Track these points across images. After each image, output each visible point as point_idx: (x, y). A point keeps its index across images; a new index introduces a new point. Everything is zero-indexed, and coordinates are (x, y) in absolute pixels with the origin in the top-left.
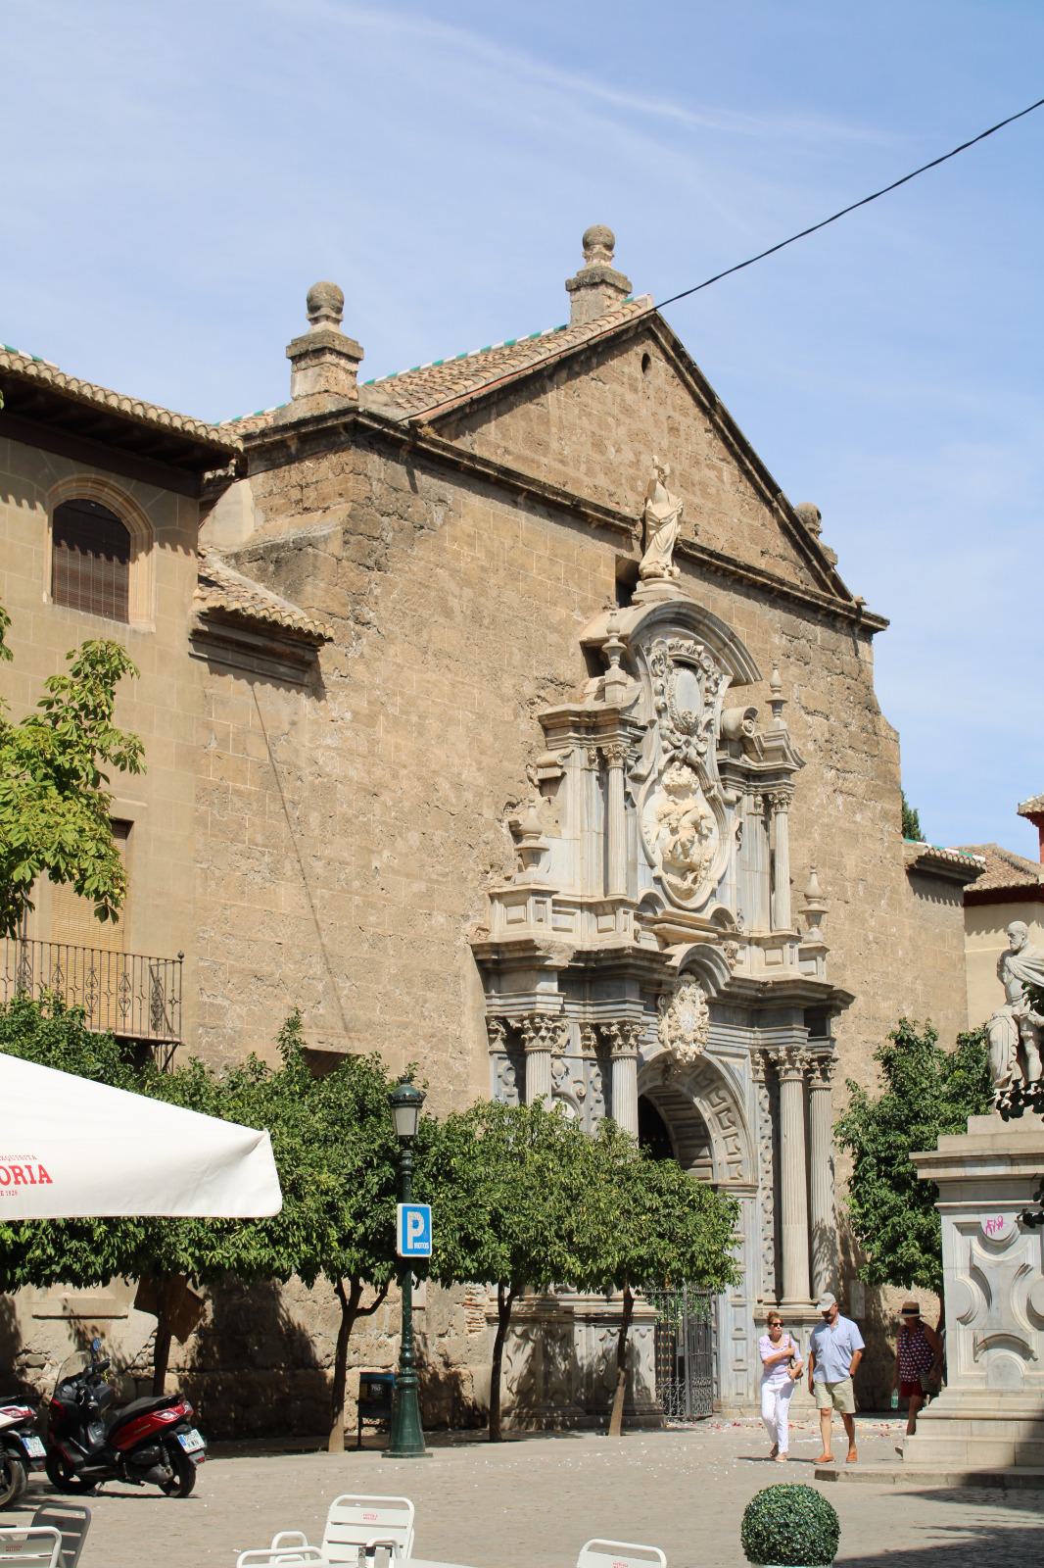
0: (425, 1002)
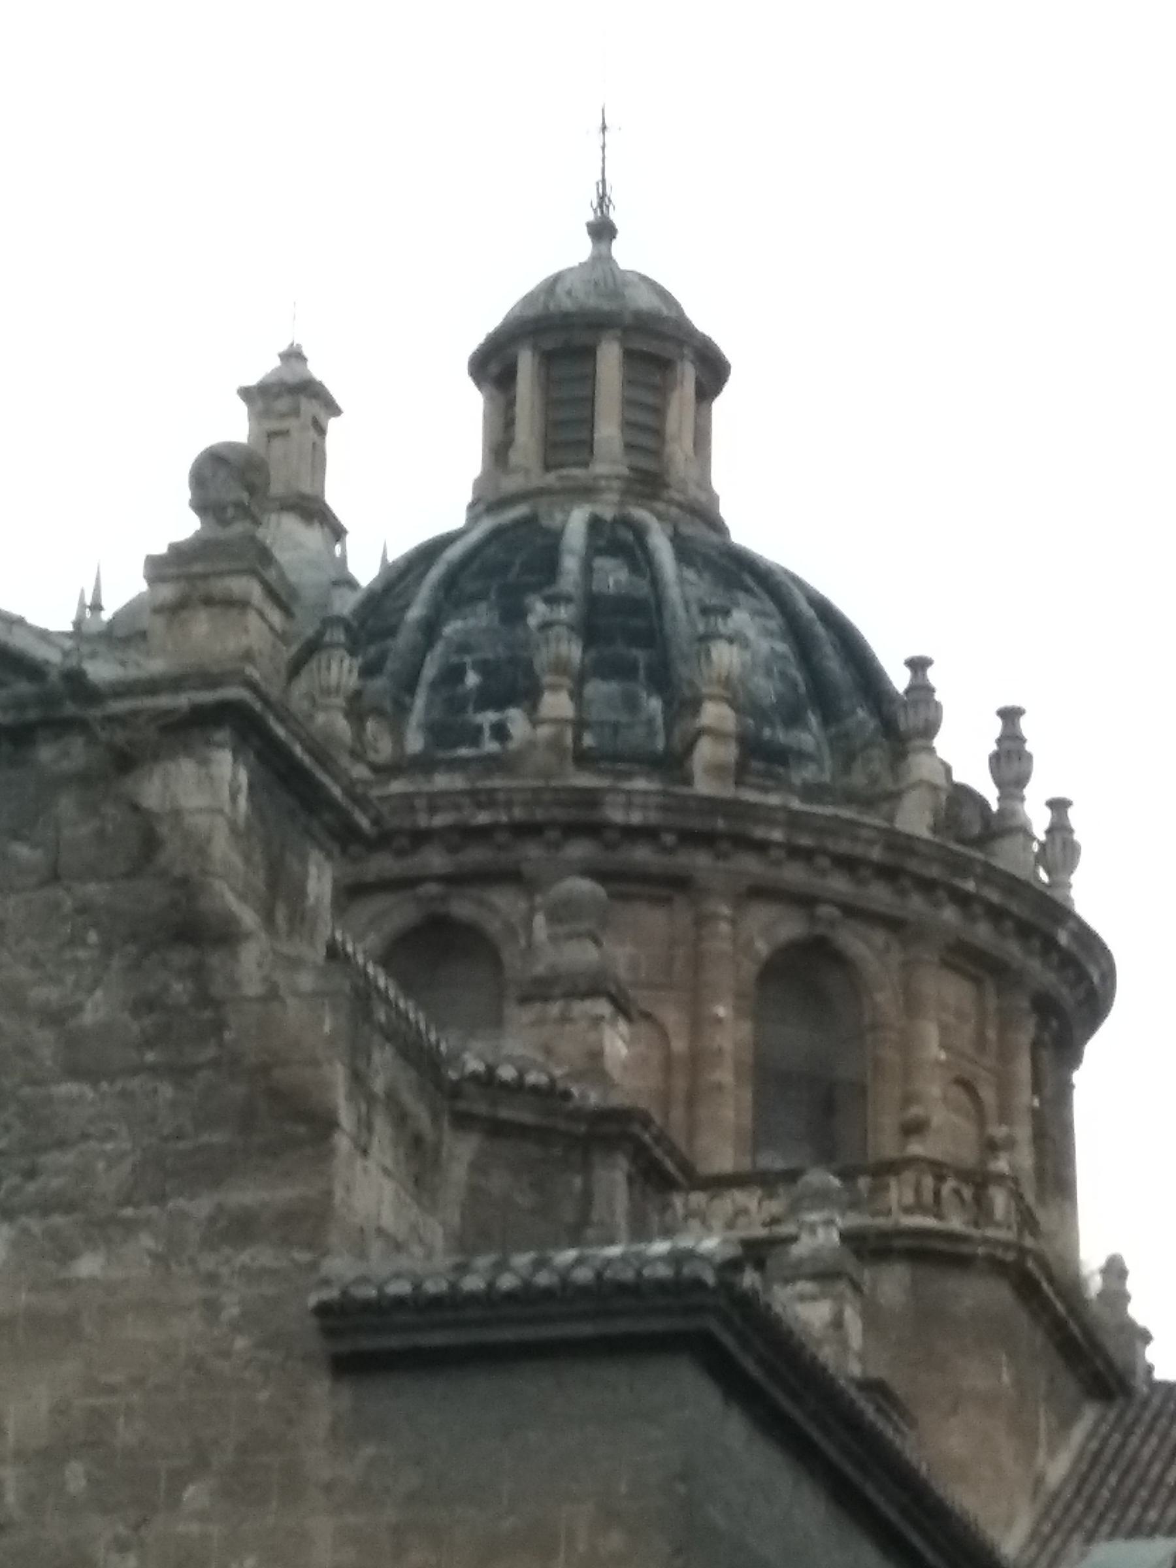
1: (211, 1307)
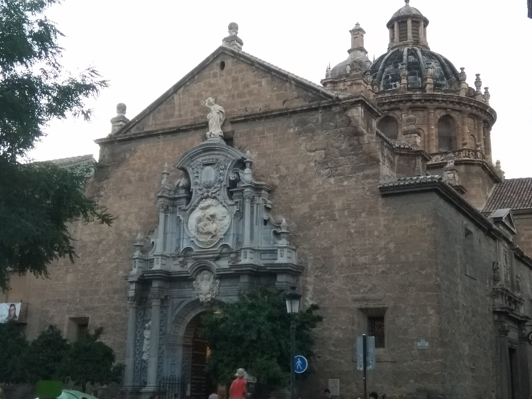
0: (114, 298)
1: (364, 188)
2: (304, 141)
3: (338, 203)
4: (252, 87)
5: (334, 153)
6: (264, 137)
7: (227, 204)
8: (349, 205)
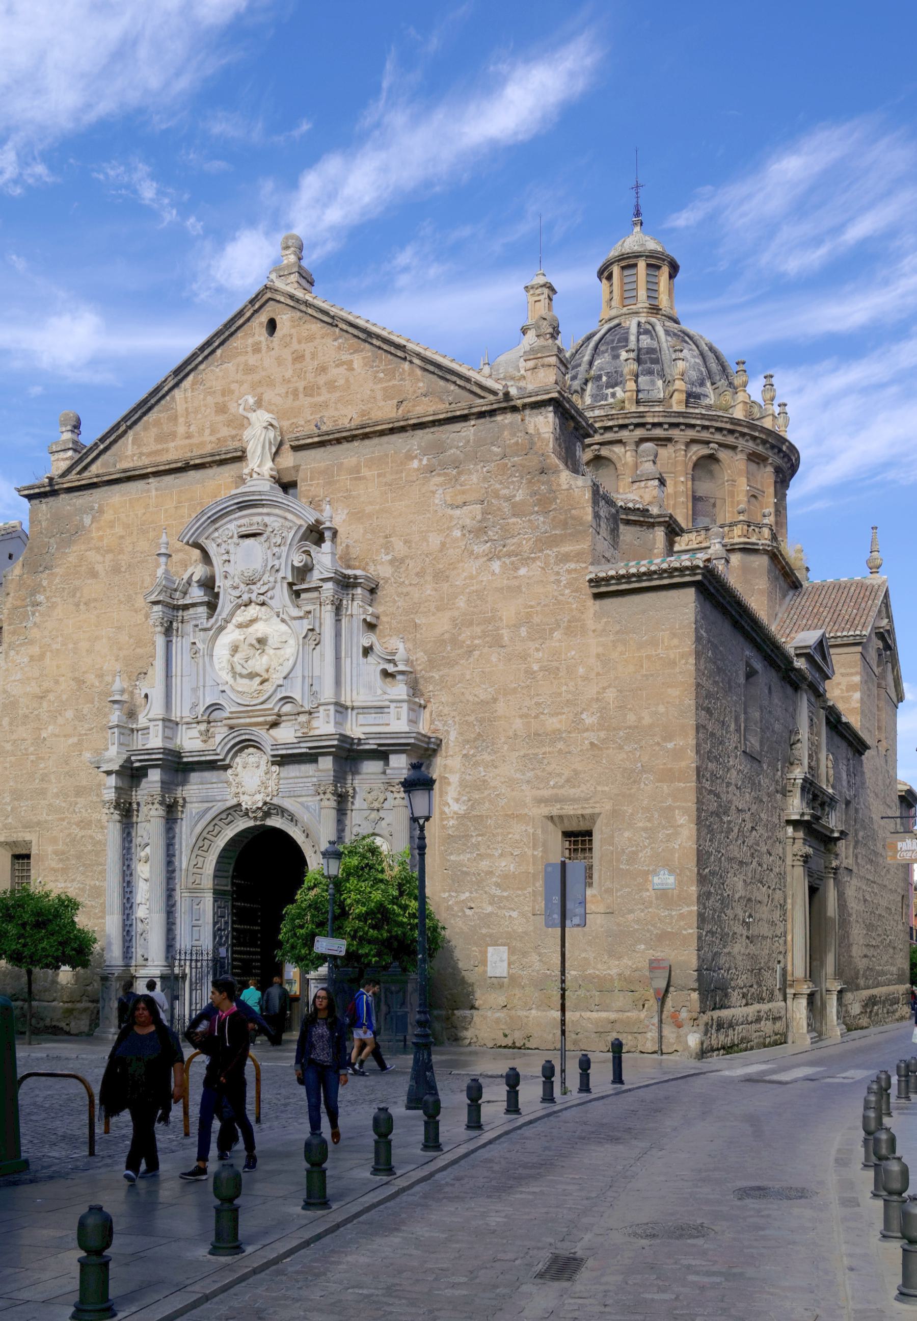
0: (76, 804)
1: (558, 581)
2: (441, 485)
3: (509, 611)
4: (334, 372)
5: (499, 509)
6: (360, 479)
7: (289, 616)
8: (529, 615)
